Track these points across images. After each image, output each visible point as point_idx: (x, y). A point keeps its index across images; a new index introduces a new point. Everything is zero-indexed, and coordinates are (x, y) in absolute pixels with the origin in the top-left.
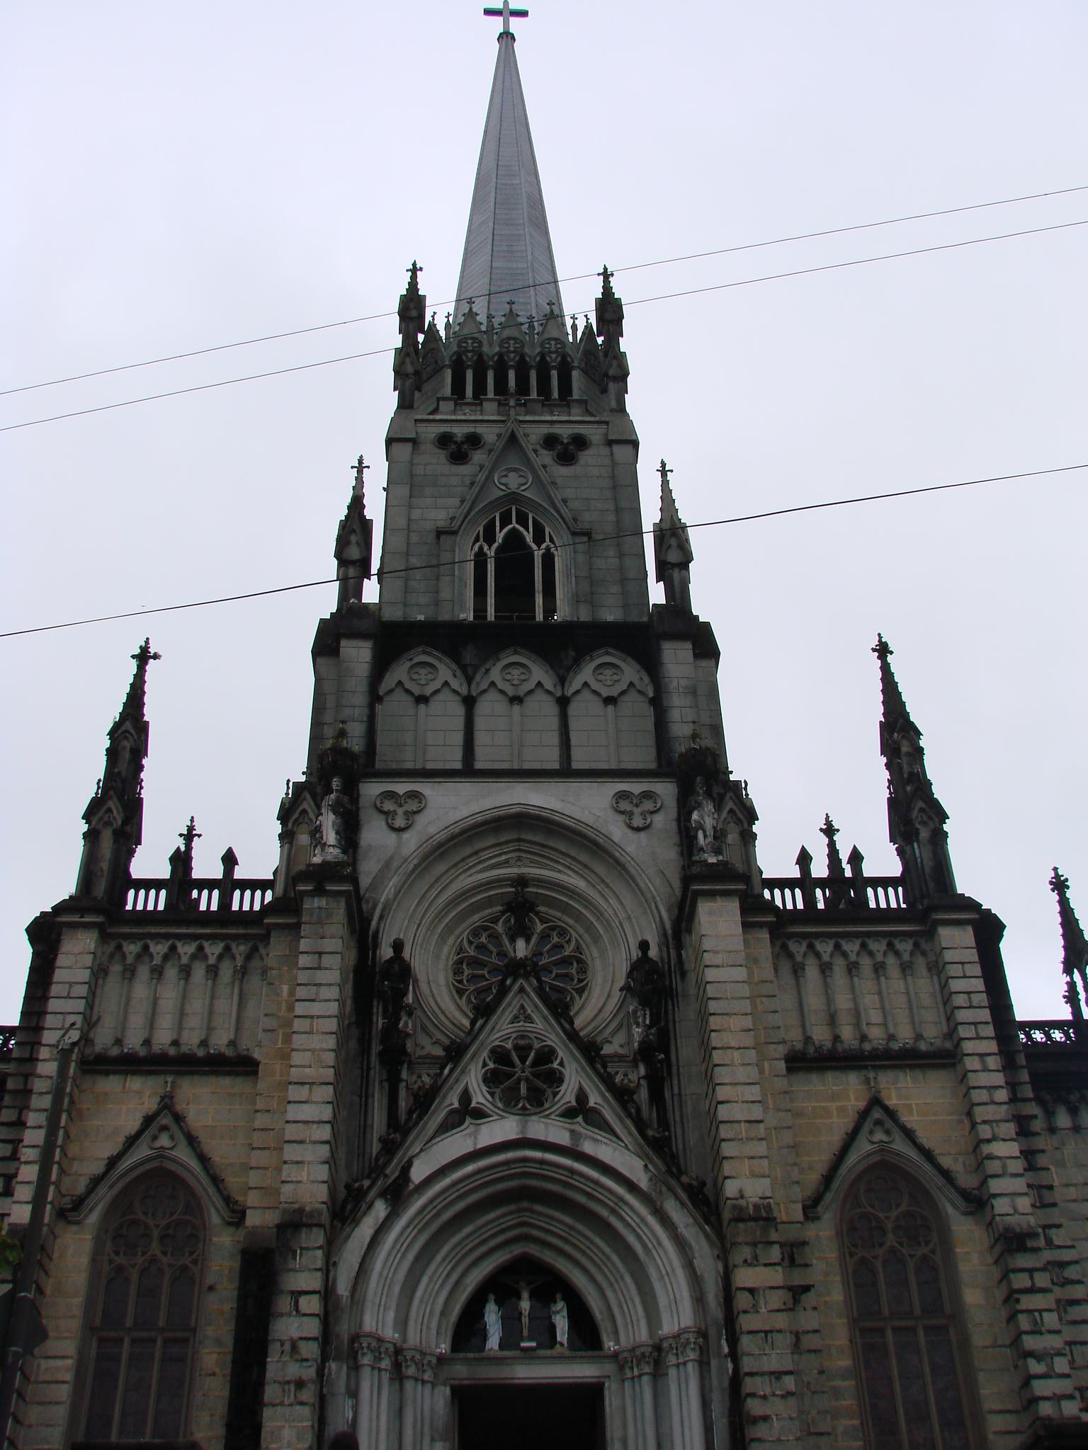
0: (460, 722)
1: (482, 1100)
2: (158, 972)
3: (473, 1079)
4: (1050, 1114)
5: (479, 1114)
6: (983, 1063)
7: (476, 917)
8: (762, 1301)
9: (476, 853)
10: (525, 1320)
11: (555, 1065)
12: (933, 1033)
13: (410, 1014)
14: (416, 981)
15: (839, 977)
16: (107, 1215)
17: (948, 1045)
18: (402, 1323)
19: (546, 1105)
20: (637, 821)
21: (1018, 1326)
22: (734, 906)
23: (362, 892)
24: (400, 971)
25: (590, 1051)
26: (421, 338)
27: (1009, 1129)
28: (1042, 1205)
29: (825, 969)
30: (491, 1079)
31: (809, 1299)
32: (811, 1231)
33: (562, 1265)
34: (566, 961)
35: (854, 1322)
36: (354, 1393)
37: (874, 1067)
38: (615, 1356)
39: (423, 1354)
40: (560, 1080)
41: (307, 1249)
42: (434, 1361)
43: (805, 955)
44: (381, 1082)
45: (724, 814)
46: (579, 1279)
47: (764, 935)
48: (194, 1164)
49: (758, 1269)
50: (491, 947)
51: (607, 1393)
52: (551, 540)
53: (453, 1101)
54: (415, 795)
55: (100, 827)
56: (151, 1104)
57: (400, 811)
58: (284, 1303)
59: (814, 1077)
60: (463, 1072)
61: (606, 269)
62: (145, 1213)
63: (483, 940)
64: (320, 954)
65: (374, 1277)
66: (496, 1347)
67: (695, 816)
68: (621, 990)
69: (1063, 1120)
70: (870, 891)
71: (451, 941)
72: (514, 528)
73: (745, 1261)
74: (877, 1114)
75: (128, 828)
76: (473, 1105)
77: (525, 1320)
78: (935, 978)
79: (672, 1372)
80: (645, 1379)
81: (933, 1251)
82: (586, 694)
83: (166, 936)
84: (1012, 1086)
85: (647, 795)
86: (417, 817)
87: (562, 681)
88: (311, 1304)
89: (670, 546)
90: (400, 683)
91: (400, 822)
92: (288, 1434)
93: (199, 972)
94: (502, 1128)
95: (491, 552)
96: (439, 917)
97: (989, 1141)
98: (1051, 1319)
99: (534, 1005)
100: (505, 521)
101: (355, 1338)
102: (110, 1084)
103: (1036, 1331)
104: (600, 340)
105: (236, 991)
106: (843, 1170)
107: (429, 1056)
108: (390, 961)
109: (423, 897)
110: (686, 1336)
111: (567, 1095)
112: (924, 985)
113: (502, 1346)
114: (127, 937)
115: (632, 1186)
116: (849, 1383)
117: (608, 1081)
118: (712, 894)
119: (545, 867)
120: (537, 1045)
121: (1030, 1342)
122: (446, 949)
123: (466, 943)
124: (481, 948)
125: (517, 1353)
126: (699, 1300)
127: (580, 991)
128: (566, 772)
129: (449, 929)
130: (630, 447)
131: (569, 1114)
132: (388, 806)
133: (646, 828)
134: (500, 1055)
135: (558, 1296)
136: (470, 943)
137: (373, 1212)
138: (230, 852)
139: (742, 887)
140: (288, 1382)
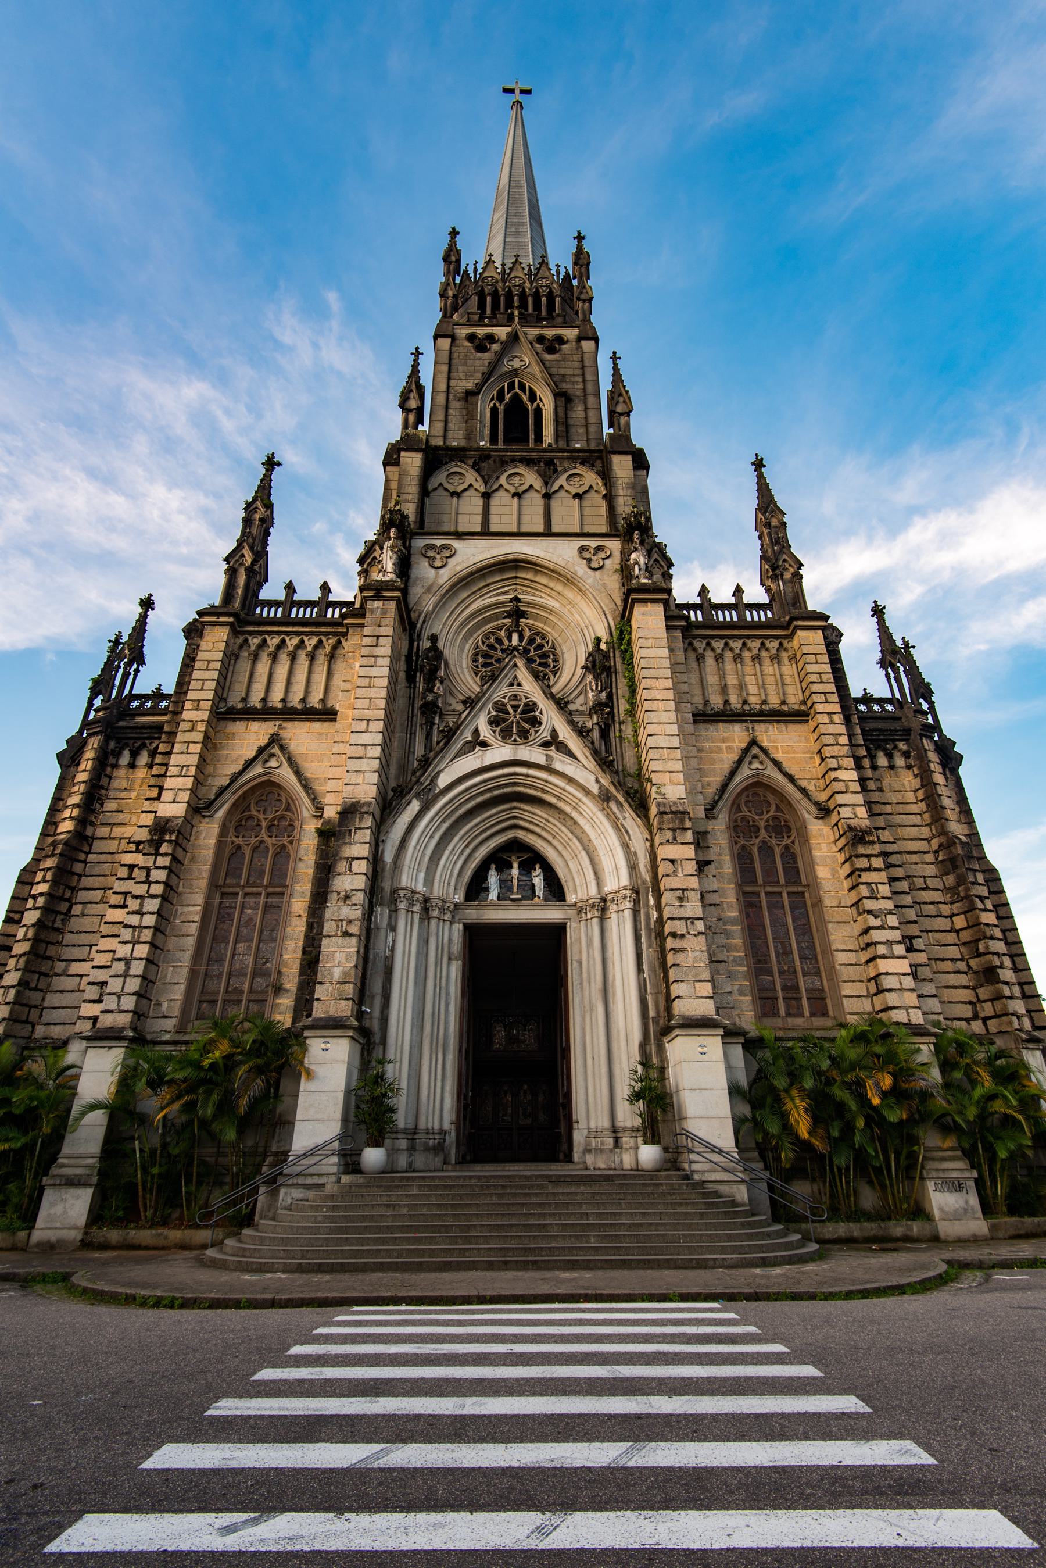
0: (479, 509)
1: (488, 735)
2: (274, 658)
4: (872, 757)
5: (484, 744)
6: (831, 719)
7: (488, 626)
8: (680, 870)
9: (488, 585)
10: (515, 882)
11: (537, 713)
12: (794, 701)
13: (442, 682)
14: (447, 665)
15: (729, 666)
16: (230, 812)
17: (803, 708)
18: (429, 881)
19: (531, 739)
20: (595, 565)
21: (859, 893)
22: (659, 609)
23: (411, 606)
24: (436, 654)
25: (561, 704)
26: (458, 280)
27: (850, 762)
28: (872, 814)
29: (719, 658)
30: (493, 722)
31: (711, 870)
32: (711, 826)
33: (539, 844)
34: (545, 656)
35: (740, 887)
36: (393, 928)
37: (752, 721)
38: (575, 905)
39: (444, 902)
40: (540, 723)
41: (360, 829)
42: (452, 907)
43: (705, 650)
44: (421, 725)
45: (652, 562)
46: (550, 854)
47: (678, 634)
48: (292, 778)
49: (676, 846)
50: (497, 645)
51: (568, 930)
52: (541, 400)
53: (468, 736)
54: (446, 547)
55: (236, 566)
56: (264, 740)
57: (438, 557)
58: (342, 866)
59: (711, 728)
60: (475, 716)
61: (579, 233)
62: (259, 811)
63: (492, 640)
64: (378, 637)
65: (410, 849)
66: (495, 898)
67: (633, 556)
68: (582, 668)
69: (882, 761)
70: (748, 613)
71: (470, 641)
72: (516, 393)
73: (668, 841)
74: (755, 750)
75: (256, 568)
76: (482, 737)
77: (515, 882)
78: (794, 665)
79: (614, 916)
80: (595, 920)
81: (793, 842)
82: (562, 493)
83: (279, 633)
84: (850, 736)
85: (599, 548)
86: (449, 560)
87: (546, 484)
88: (361, 866)
89: (618, 402)
90: (441, 485)
91: (438, 563)
92: (339, 956)
93: (302, 656)
94: (500, 752)
95: (501, 408)
96: (463, 625)
97: (835, 769)
98: (884, 890)
99: (523, 674)
100: (511, 386)
101: (395, 891)
102: (239, 727)
103: (873, 897)
104: (575, 282)
105: (325, 668)
106: (731, 786)
107: (454, 710)
108: (429, 649)
109: (452, 612)
110: (624, 892)
111: (545, 734)
112: (789, 670)
113: (499, 898)
114: (251, 633)
115: (587, 792)
116: (737, 928)
117: (571, 723)
118: (645, 601)
119: (532, 595)
120: (524, 700)
121: (869, 904)
122: (467, 646)
123: (480, 643)
124: (491, 646)
125: (509, 902)
126: (633, 868)
127: (555, 674)
128: (548, 533)
129: (470, 633)
130: (592, 343)
131: (546, 745)
132: (431, 553)
133: (601, 568)
134: (500, 707)
135: (537, 866)
136: (483, 643)
137: (410, 808)
138: (325, 583)
139: (666, 596)
140: (342, 921)
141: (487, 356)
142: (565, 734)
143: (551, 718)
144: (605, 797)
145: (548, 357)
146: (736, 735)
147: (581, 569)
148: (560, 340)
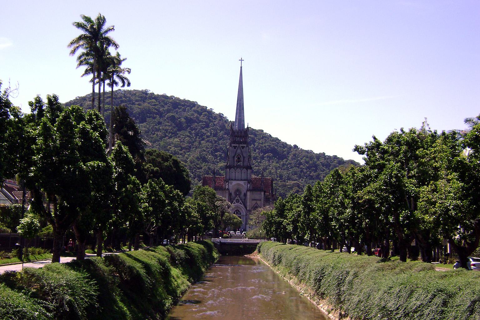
25: (241, 200)
94: (237, 204)
128: (241, 180)
142: (241, 203)
146: (255, 201)
147: (244, 185)
148: (244, 147)
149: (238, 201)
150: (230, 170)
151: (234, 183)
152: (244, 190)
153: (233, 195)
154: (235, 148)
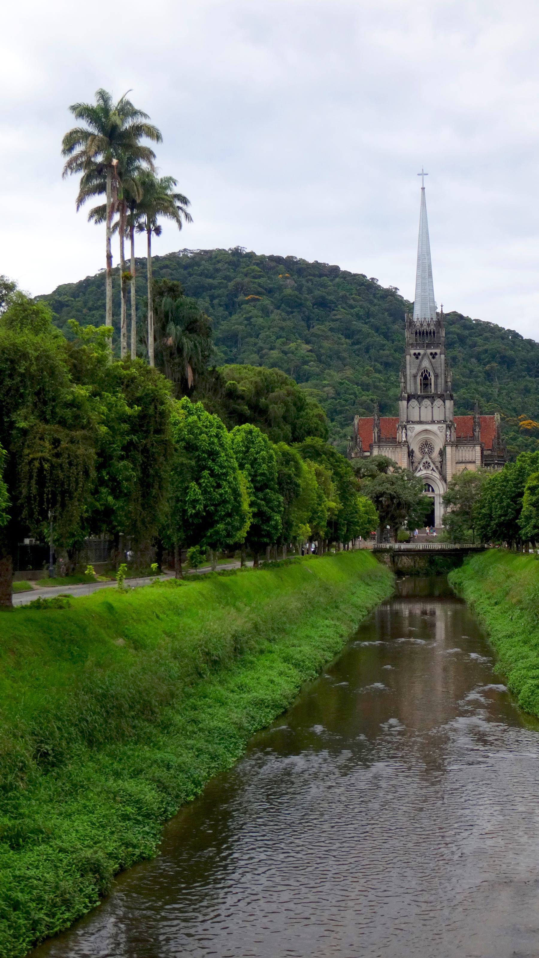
3: (421, 466)
12: (474, 459)
24: (413, 452)
25: (434, 464)
94: (424, 472)
111: (431, 468)
112: (474, 452)
128: (433, 422)
141: (418, 361)
142: (435, 469)
143: (432, 466)
144: (440, 480)
145: (433, 360)
146: (462, 466)
147: (438, 432)
148: (436, 354)
149: (427, 466)
150: (408, 403)
151: (418, 428)
152: (438, 446)
153: (418, 454)
154: (417, 358)
